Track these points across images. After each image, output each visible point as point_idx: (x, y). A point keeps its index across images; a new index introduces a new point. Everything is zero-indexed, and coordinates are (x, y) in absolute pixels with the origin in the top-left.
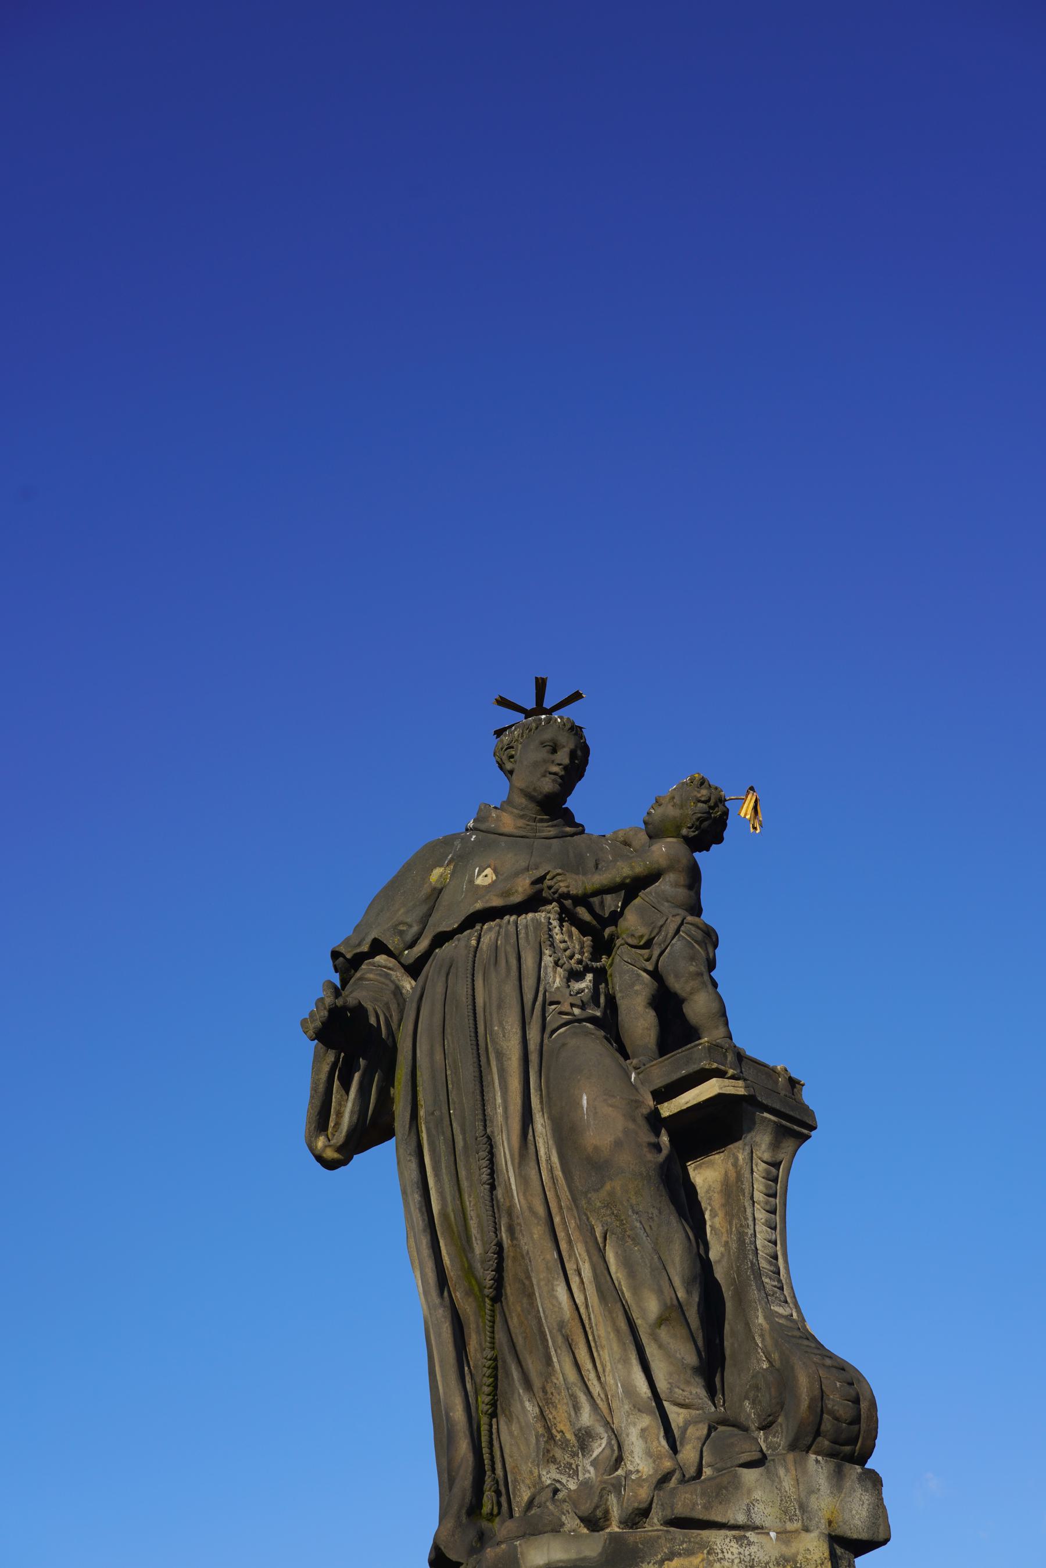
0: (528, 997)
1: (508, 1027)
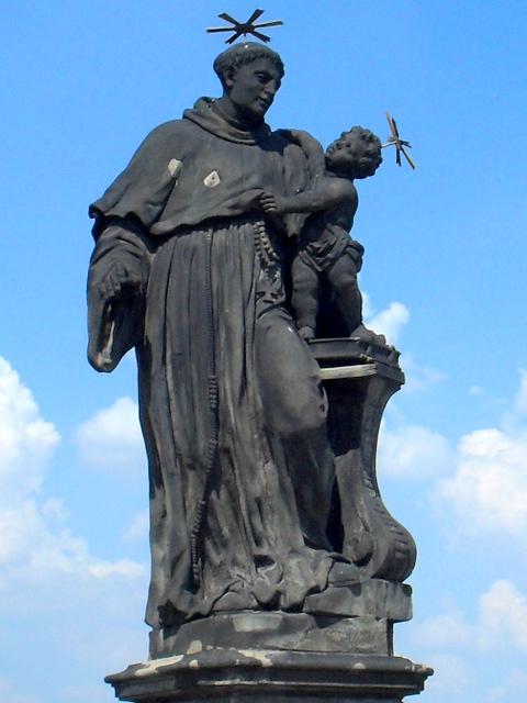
0: (247, 288)
1: (235, 310)
